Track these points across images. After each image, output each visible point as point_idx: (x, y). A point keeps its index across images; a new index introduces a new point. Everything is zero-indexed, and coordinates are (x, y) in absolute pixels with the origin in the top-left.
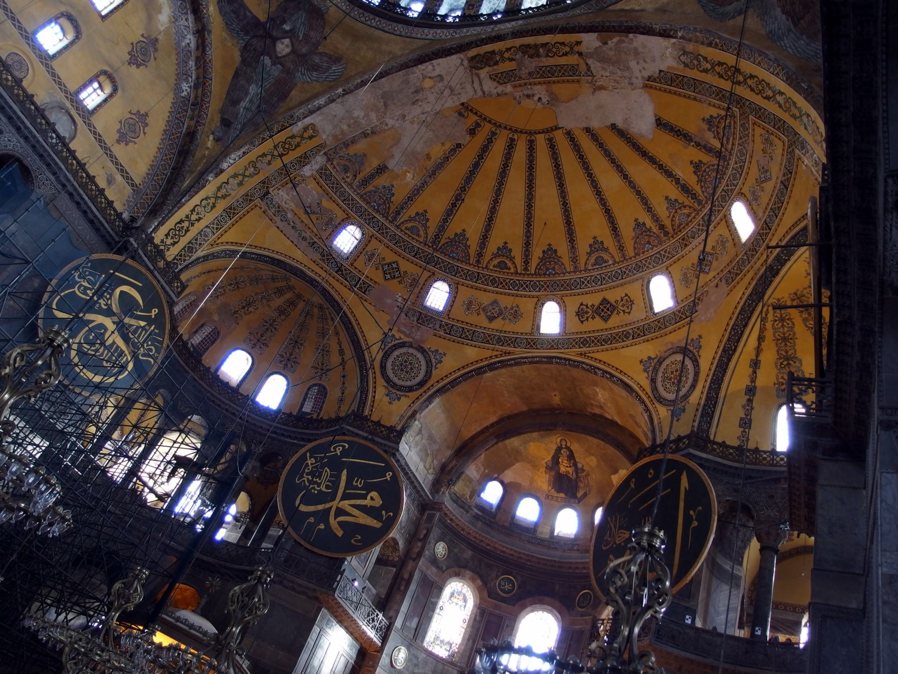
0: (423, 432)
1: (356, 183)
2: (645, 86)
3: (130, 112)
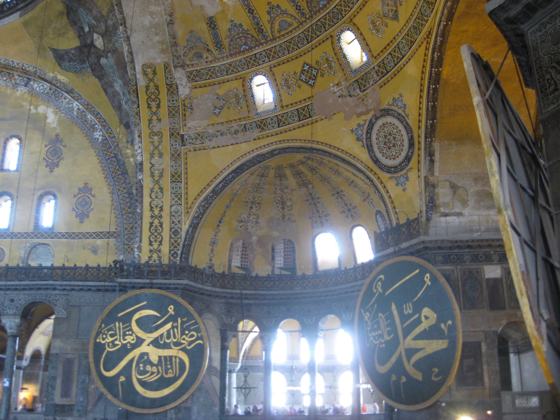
0: (460, 184)
1: (216, 53)
3: (75, 196)
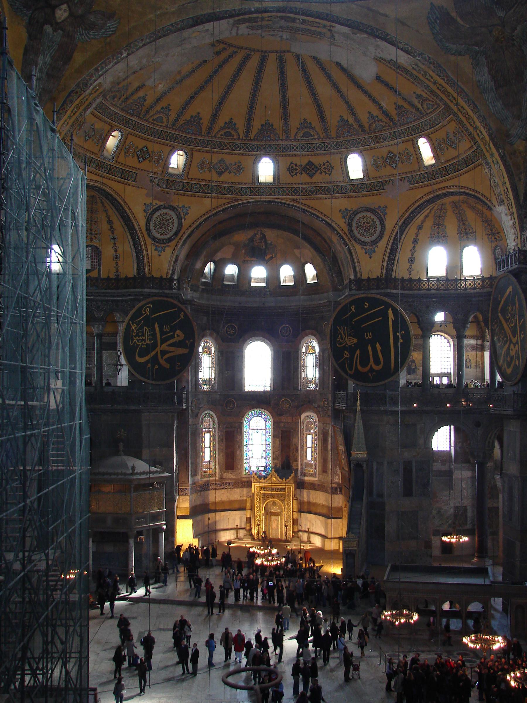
1: (120, 102)
2: (374, 58)
